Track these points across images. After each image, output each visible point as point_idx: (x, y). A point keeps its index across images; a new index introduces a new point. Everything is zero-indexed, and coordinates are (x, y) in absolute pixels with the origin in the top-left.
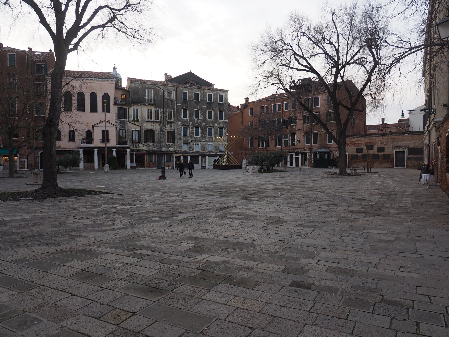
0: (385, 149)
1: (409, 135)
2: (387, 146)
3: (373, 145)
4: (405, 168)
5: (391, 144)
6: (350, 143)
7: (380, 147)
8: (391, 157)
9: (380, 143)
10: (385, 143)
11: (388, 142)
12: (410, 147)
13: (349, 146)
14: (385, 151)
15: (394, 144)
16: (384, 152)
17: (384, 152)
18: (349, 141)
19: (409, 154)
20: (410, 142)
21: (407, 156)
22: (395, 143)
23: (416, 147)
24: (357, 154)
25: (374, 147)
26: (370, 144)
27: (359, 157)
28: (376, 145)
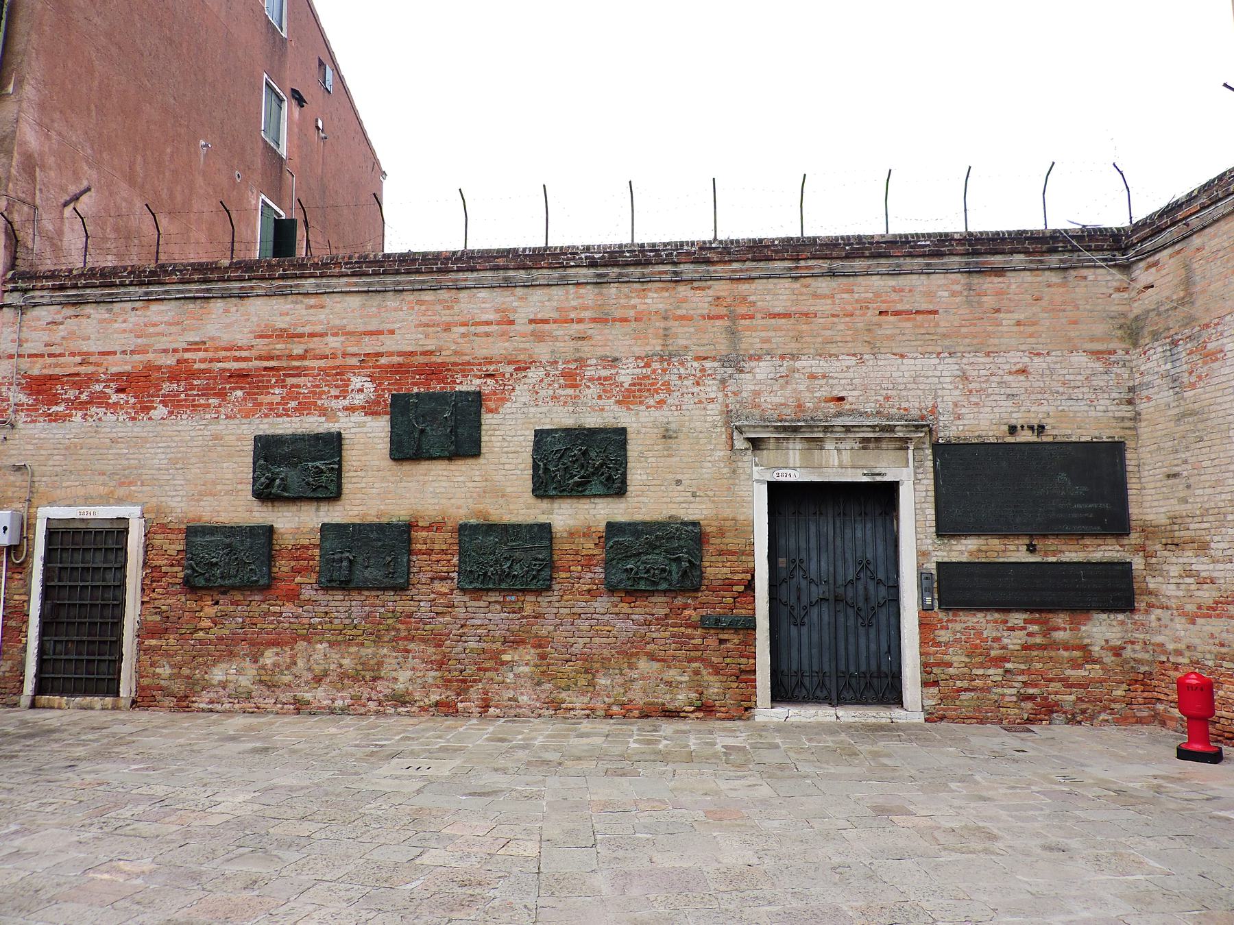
0: (634, 449)
1: (938, 280)
2: (661, 416)
3: (477, 398)
4: (897, 714)
5: (711, 388)
6: (174, 376)
7: (567, 431)
8: (715, 569)
9: (571, 378)
10: (626, 375)
11: (666, 358)
12: (950, 430)
13: (160, 411)
14: (636, 475)
15: (747, 383)
16: (617, 488)
17: (617, 488)
18: (164, 343)
19: (946, 528)
20: (949, 368)
21: (922, 554)
22: (763, 370)
23: (1026, 437)
24: (261, 515)
25: (488, 420)
26: (436, 387)
27: (283, 566)
28: (521, 394)
